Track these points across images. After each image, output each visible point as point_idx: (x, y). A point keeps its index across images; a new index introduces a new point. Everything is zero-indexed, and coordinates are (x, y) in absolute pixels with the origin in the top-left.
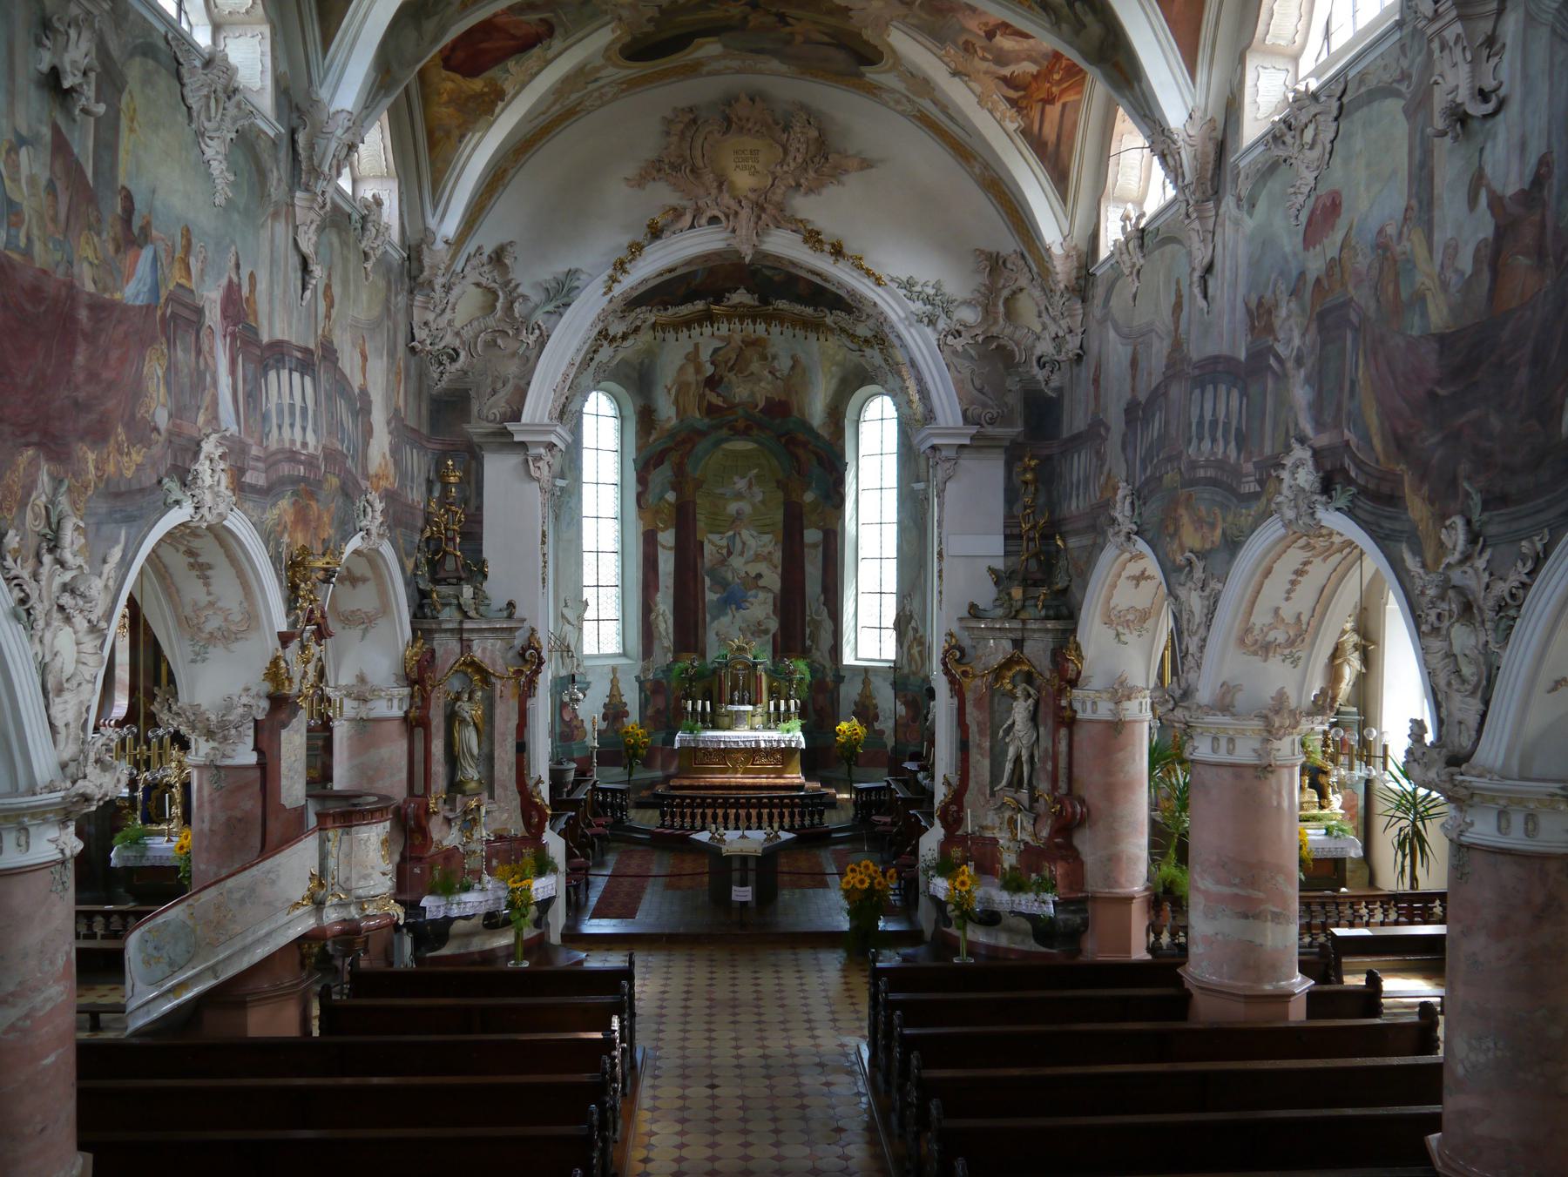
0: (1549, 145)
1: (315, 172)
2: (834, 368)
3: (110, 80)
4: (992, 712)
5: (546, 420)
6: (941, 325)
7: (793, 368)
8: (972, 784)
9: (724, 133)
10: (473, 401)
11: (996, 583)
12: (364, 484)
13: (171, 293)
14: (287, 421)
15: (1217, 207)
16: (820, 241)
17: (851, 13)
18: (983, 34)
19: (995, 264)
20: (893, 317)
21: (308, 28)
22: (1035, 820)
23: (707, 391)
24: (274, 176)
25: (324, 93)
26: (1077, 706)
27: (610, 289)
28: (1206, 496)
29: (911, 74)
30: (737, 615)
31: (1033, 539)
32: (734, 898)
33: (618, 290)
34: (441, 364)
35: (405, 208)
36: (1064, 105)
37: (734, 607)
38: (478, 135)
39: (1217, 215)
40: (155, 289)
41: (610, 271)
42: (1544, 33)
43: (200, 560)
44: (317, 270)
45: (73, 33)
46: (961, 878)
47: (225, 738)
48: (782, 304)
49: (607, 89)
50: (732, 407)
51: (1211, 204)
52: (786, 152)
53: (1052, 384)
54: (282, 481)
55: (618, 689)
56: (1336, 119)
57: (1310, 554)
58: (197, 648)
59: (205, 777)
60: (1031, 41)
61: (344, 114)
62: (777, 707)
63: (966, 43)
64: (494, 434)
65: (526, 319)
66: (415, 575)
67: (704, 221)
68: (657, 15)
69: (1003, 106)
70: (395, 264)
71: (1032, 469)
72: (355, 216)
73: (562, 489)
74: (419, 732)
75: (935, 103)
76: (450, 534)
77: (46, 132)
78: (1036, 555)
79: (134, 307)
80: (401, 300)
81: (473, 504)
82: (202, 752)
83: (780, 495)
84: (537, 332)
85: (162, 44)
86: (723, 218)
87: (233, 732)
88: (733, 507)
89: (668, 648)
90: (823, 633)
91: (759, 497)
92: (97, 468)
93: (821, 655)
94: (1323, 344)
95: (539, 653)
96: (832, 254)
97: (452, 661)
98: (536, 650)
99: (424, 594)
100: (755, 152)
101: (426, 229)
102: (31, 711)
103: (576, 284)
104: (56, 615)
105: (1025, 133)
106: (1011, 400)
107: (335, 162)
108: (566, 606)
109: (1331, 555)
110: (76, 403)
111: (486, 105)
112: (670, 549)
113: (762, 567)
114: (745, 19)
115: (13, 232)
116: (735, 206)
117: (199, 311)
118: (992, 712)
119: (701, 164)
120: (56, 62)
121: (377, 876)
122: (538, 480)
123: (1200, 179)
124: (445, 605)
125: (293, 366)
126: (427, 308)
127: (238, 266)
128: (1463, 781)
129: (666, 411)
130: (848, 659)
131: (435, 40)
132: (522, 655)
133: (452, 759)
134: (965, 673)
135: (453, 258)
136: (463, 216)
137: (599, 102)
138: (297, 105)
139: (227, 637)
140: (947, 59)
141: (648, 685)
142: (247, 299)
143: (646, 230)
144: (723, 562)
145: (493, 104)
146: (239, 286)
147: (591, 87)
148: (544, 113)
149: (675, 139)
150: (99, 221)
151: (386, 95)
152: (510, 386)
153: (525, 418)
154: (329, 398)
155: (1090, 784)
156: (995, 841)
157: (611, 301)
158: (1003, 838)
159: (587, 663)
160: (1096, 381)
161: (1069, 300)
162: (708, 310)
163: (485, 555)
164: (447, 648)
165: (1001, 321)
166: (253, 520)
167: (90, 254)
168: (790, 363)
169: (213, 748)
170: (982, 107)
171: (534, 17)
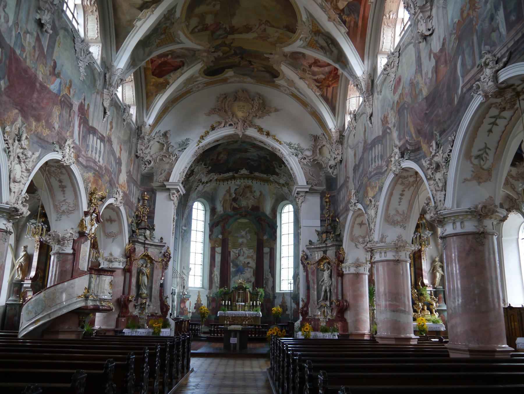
0: (445, 34)
1: (111, 85)
2: (273, 195)
4: (317, 276)
5: (177, 182)
6: (300, 156)
7: (260, 195)
8: (311, 301)
9: (234, 101)
10: (155, 176)
11: (318, 235)
12: (117, 185)
13: (64, 95)
14: (94, 151)
15: (373, 97)
16: (263, 131)
17: (270, 60)
19: (316, 138)
20: (285, 154)
21: (112, 42)
22: (332, 311)
23: (233, 202)
24: (98, 83)
25: (115, 64)
26: (344, 270)
27: (198, 144)
28: (374, 179)
29: (289, 80)
30: (241, 276)
31: (329, 220)
32: (231, 342)
33: (201, 145)
34: (145, 164)
35: (138, 115)
36: (333, 88)
37: (240, 273)
38: (161, 95)
39: (373, 100)
40: (59, 91)
41: (198, 139)
42: (441, 9)
43: (63, 184)
44: (108, 113)
45: (46, 11)
46: (306, 327)
47: (64, 244)
48: (257, 174)
49: (199, 85)
50: (241, 208)
51: (371, 97)
52: (253, 106)
53: (334, 174)
54: (91, 167)
55: (200, 299)
56: (399, 57)
57: (403, 187)
58: (58, 216)
59: (56, 257)
60: (322, 68)
61: (121, 69)
62: (253, 304)
63: (303, 69)
66: (132, 225)
67: (228, 125)
68: (214, 60)
69: (315, 88)
70: (133, 129)
71: (328, 198)
72: (122, 107)
73: (185, 230)
74: (128, 275)
75: (296, 88)
76: (144, 215)
78: (330, 224)
79: (52, 92)
80: (134, 140)
81: (152, 207)
82: (55, 250)
83: (256, 237)
84: (176, 156)
86: (233, 124)
87: (66, 242)
88: (240, 240)
89: (218, 286)
90: (269, 282)
91: (249, 237)
92: (35, 127)
93: (269, 290)
94: (400, 118)
95: (170, 255)
96: (266, 135)
99: (134, 232)
100: (244, 106)
101: (144, 121)
102: (4, 173)
104: (16, 159)
105: (322, 96)
106: (321, 178)
107: (116, 83)
109: (410, 187)
110: (32, 106)
111: (164, 86)
112: (220, 253)
113: (249, 260)
114: (240, 62)
115: (22, 52)
116: (238, 122)
117: (72, 105)
118: (317, 276)
119: (227, 109)
120: (41, 17)
121: (106, 293)
122: (173, 200)
123: (367, 90)
124: (140, 235)
126: (142, 145)
127: (84, 100)
128: (440, 213)
129: (219, 208)
130: (277, 291)
132: (164, 255)
133: (138, 286)
134: (308, 263)
135: (151, 131)
136: (155, 118)
137: (197, 90)
138: (107, 67)
139: (68, 212)
141: (210, 298)
142: (86, 110)
143: (211, 127)
144: (237, 258)
147: (195, 83)
148: (181, 90)
149: (220, 102)
151: (134, 67)
152: (166, 172)
153: (170, 181)
154: (108, 153)
155: (349, 297)
156: (319, 320)
157: (199, 148)
158: (322, 318)
159: (190, 289)
160: (346, 166)
161: (337, 145)
162: (234, 175)
163: (155, 223)
164: (140, 250)
165: (318, 155)
167: (43, 71)
168: (259, 193)
169: (59, 248)
170: (309, 88)
171: (178, 60)
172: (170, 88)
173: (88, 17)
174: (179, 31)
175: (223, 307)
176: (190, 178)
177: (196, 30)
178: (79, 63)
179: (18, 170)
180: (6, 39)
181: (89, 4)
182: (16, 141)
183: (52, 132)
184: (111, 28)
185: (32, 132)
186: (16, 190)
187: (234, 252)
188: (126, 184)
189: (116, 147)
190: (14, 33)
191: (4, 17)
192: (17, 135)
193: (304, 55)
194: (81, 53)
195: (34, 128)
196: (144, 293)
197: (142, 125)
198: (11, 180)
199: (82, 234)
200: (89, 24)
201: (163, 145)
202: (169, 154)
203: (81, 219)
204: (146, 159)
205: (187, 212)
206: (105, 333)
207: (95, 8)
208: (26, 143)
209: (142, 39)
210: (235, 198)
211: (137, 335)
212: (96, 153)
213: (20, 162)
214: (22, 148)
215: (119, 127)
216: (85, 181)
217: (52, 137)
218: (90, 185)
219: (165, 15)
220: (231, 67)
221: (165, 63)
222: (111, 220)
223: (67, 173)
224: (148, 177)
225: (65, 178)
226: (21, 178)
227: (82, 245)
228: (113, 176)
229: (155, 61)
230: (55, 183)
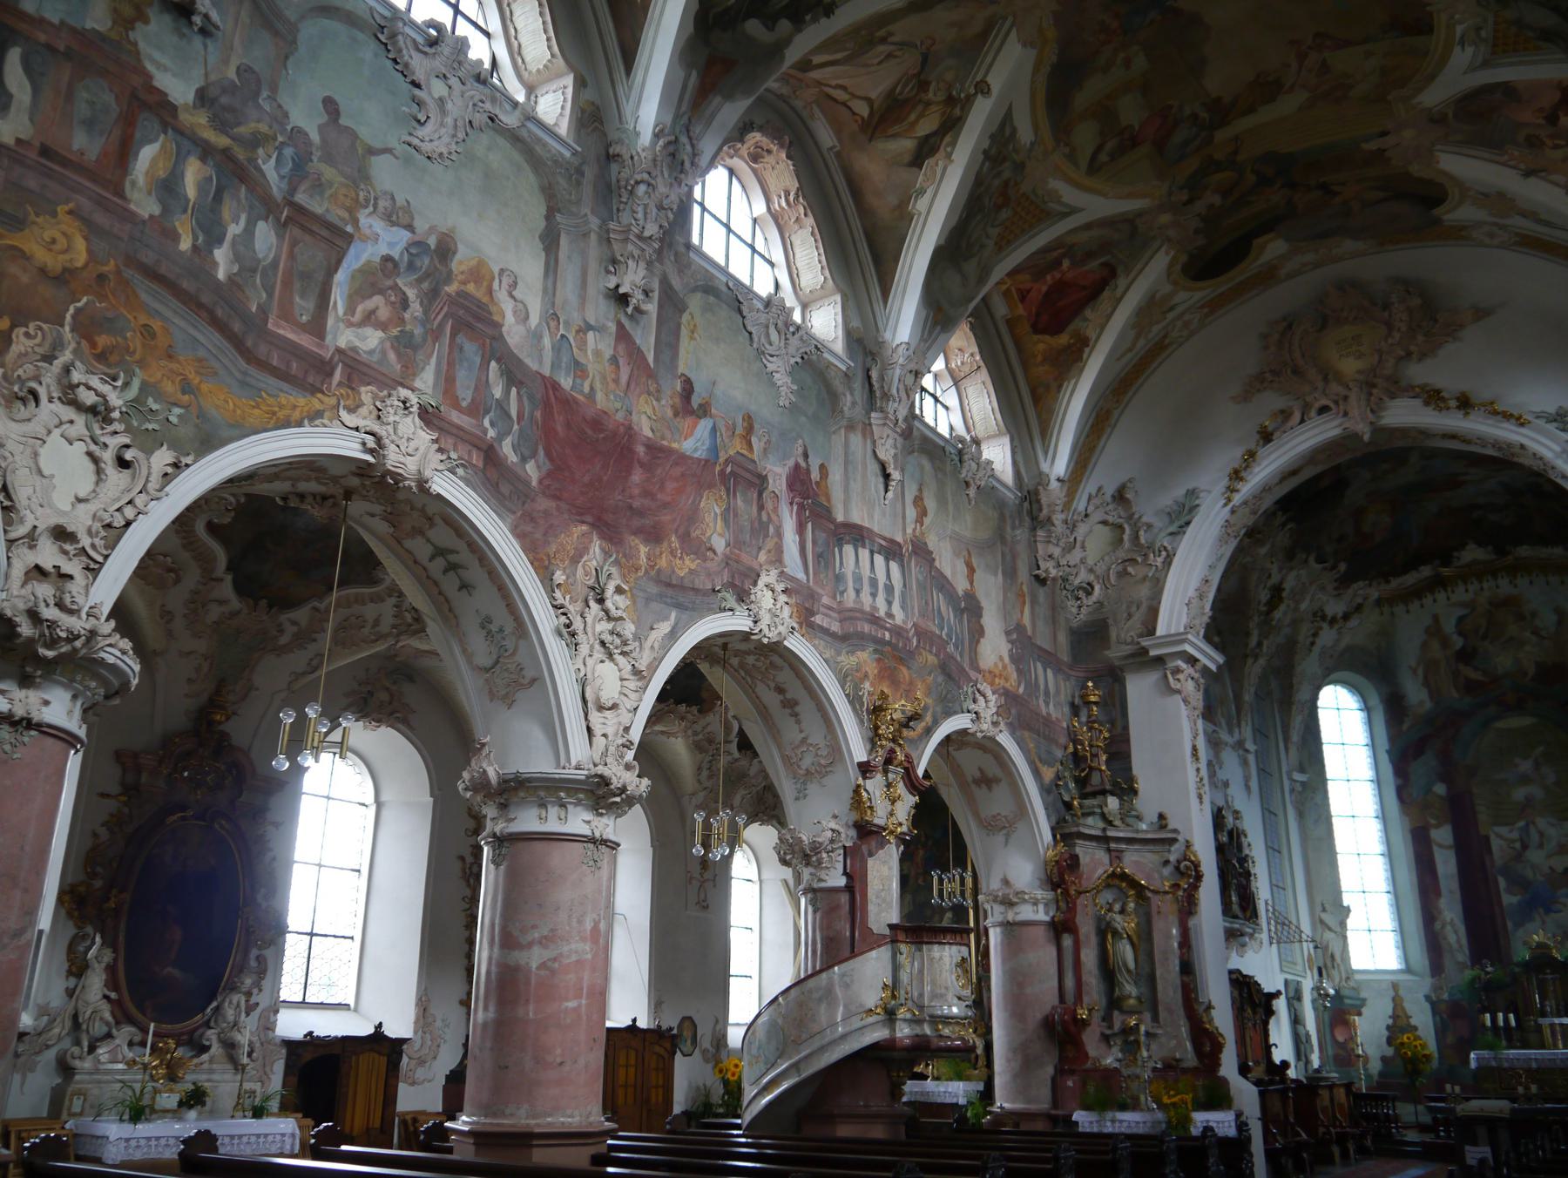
1: (886, 396)
3: (672, 303)
5: (1182, 630)
12: (973, 675)
14: (866, 589)
16: (1443, 399)
18: (1543, 122)
20: (1548, 455)
23: (1461, 667)
25: (888, 336)
27: (1229, 500)
33: (1237, 499)
34: (1078, 599)
35: (1020, 458)
37: (1541, 910)
38: (1073, 382)
40: (714, 449)
41: (1225, 482)
43: (789, 696)
44: (896, 475)
45: (630, 262)
47: (820, 862)
48: (1524, 551)
49: (1187, 317)
52: (1389, 326)
54: (862, 636)
55: (1403, 1009)
64: (1132, 655)
65: (1150, 547)
66: (1057, 786)
67: (1313, 413)
72: (949, 449)
73: (1303, 783)
74: (1067, 941)
76: (1094, 750)
77: (612, 327)
79: (691, 458)
80: (1021, 534)
84: (1164, 553)
85: (724, 289)
86: (1332, 405)
87: (824, 855)
88: (1519, 794)
96: (1458, 408)
97: (1100, 871)
98: (1192, 862)
101: (1041, 474)
103: (1197, 502)
104: (597, 647)
107: (901, 387)
108: (1324, 910)
110: (630, 507)
115: (578, 381)
117: (763, 479)
121: (950, 997)
122: (1178, 692)
125: (875, 549)
126: (1049, 542)
127: (806, 456)
131: (981, 281)
133: (1108, 972)
135: (1071, 495)
140: (1512, 163)
142: (817, 483)
143: (1258, 437)
144: (1518, 857)
145: (1081, 351)
146: (808, 471)
147: (1170, 316)
148: (1130, 350)
150: (658, 391)
153: (1160, 631)
154: (921, 586)
157: (1233, 512)
159: (1357, 977)
163: (1135, 771)
164: (1094, 861)
166: (827, 656)
167: (650, 412)
171: (1094, 264)
172: (1094, 354)
173: (793, 238)
174: (1051, 180)
175: (1490, 1037)
176: (1277, 614)
177: (1103, 157)
178: (768, 365)
179: (608, 679)
180: (528, 361)
181: (784, 204)
182: (592, 603)
183: (705, 560)
184: (859, 245)
185: (640, 574)
186: (610, 731)
187: (1499, 836)
188: (1011, 669)
189: (949, 563)
190: (547, 341)
191: (515, 312)
192: (593, 588)
193: (1508, 91)
194: (768, 335)
195: (643, 560)
196: (1130, 997)
197: (1039, 484)
198: (589, 705)
199: (866, 832)
200: (798, 256)
201: (1121, 527)
202: (1143, 551)
203: (854, 787)
204: (1077, 582)
205: (1297, 722)
206: (1017, 1125)
207: (802, 210)
208: (622, 606)
209: (942, 242)
210: (1463, 648)
211: (1117, 1130)
212: (874, 595)
213: (610, 656)
214: (609, 618)
215: (951, 507)
216: (846, 676)
217: (709, 575)
218: (867, 685)
219: (985, 152)
220: (1268, 226)
221: (1060, 287)
222: (986, 781)
223: (786, 665)
224: (1091, 636)
225: (785, 676)
226: (622, 697)
227: (870, 862)
228: (951, 648)
229: (1029, 291)
230: (771, 699)
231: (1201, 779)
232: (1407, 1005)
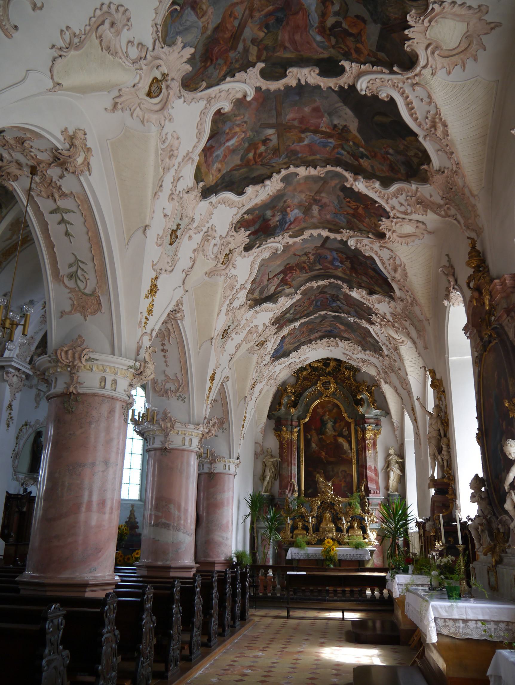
55: (134, 516)
122: (7, 381)
148: (10, 239)
153: (5, 356)
231: (11, 418)
232: (135, 513)
